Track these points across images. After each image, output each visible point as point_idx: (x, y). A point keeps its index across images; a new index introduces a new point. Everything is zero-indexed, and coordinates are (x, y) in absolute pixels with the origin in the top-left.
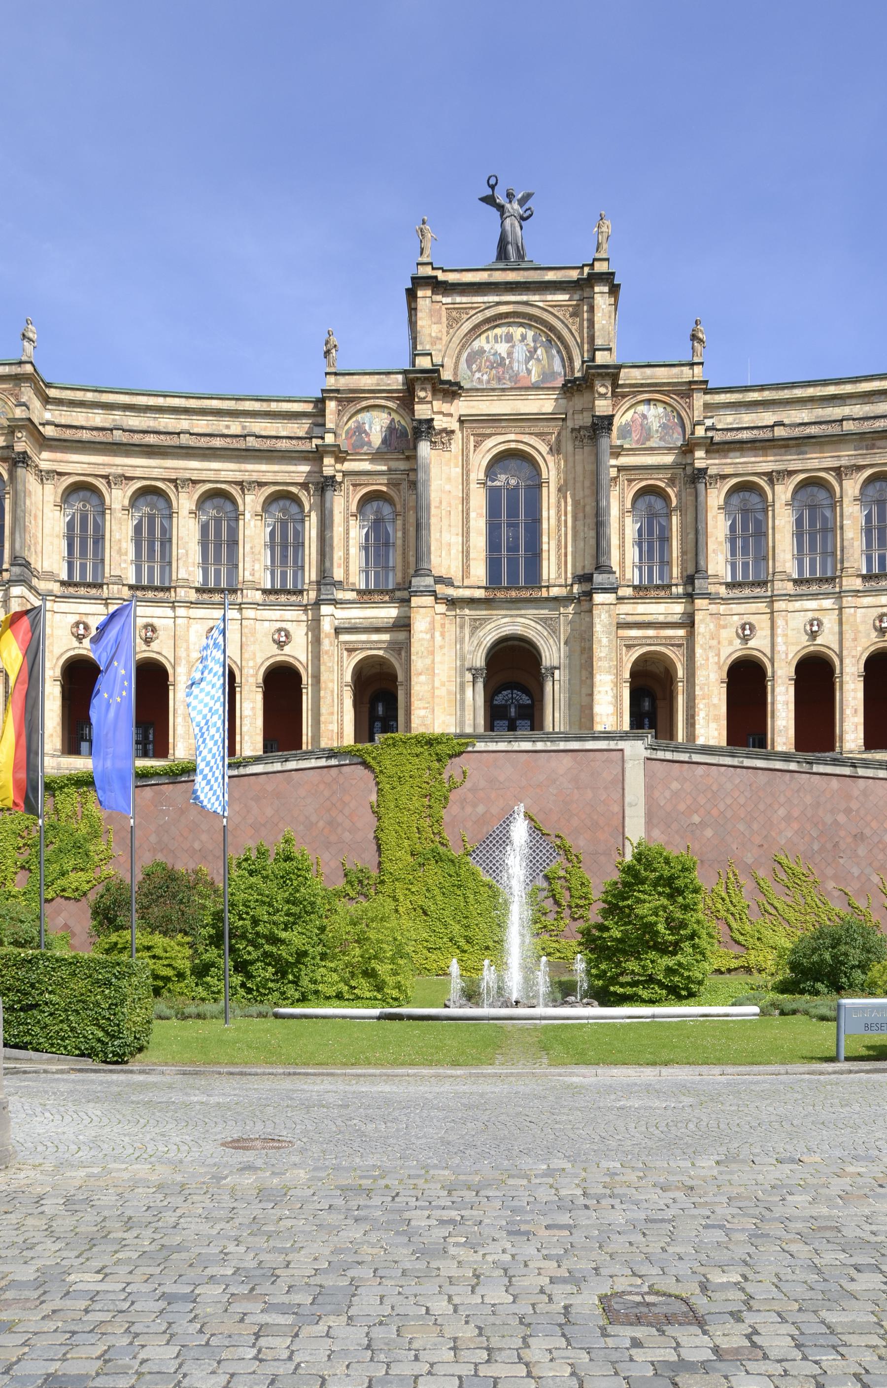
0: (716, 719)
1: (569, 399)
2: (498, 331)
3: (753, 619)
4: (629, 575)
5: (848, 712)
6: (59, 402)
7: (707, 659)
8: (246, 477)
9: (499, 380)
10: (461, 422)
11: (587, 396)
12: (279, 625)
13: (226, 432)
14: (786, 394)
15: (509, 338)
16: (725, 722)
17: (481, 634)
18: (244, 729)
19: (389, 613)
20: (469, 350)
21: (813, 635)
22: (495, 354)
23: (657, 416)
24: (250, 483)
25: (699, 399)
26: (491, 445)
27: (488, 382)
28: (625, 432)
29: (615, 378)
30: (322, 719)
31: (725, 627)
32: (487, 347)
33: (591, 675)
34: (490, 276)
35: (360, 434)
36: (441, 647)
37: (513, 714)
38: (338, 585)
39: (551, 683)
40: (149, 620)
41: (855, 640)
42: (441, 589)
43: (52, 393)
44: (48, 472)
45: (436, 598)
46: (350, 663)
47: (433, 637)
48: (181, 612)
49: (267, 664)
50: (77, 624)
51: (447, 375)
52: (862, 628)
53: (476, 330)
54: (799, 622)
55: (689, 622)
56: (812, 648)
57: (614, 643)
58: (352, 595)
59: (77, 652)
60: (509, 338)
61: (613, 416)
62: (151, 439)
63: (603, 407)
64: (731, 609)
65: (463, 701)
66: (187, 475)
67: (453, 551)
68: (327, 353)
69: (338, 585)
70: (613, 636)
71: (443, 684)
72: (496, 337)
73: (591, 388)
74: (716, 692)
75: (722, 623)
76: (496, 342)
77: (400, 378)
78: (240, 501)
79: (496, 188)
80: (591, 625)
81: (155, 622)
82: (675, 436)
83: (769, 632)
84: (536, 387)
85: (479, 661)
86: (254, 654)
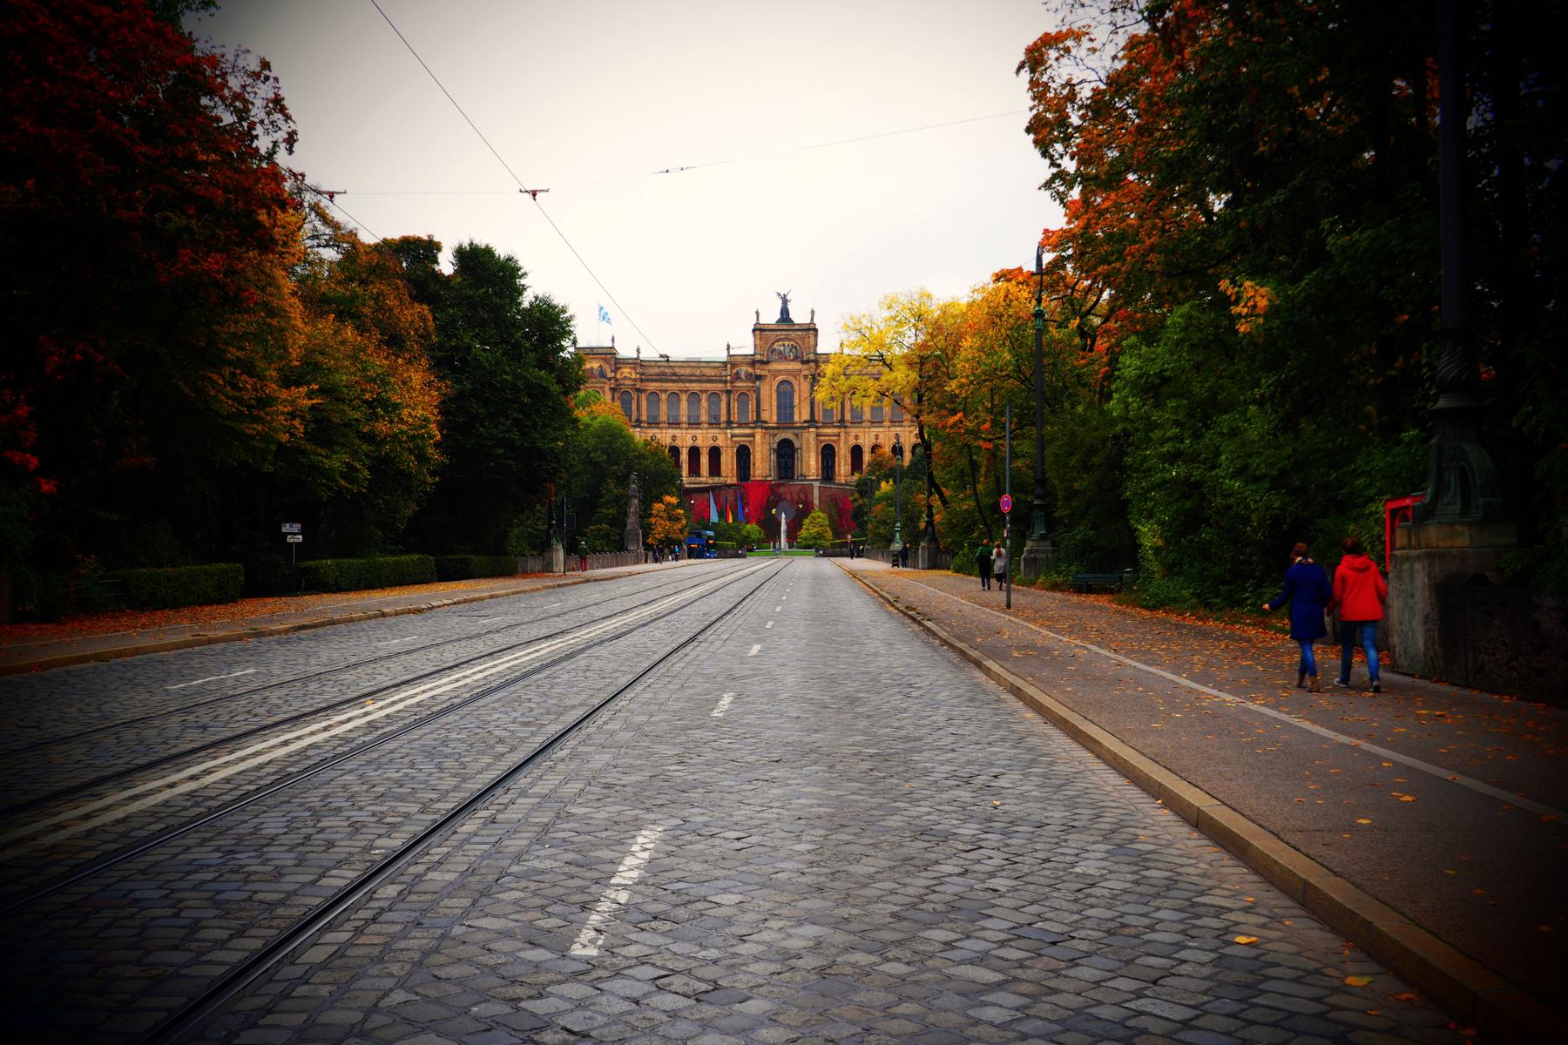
19: (747, 431)
21: (877, 439)
38: (732, 422)
53: (773, 343)
54: (872, 435)
68: (728, 349)
69: (732, 422)
85: (775, 446)
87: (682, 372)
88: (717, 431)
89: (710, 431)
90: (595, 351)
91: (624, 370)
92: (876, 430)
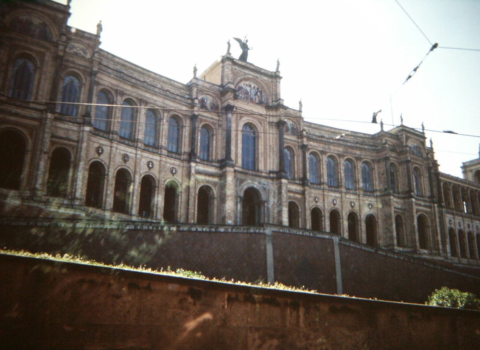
1: (267, 112)
2: (247, 83)
3: (319, 196)
9: (247, 99)
12: (172, 166)
15: (250, 86)
20: (238, 86)
21: (335, 204)
23: (290, 125)
27: (244, 98)
32: (244, 87)
34: (246, 65)
35: (203, 103)
40: (125, 153)
48: (139, 152)
53: (241, 81)
54: (330, 199)
55: (303, 193)
56: (334, 209)
60: (250, 86)
81: (128, 154)
84: (257, 104)
85: (242, 194)
88: (177, 162)
91: (76, 45)
92: (333, 194)
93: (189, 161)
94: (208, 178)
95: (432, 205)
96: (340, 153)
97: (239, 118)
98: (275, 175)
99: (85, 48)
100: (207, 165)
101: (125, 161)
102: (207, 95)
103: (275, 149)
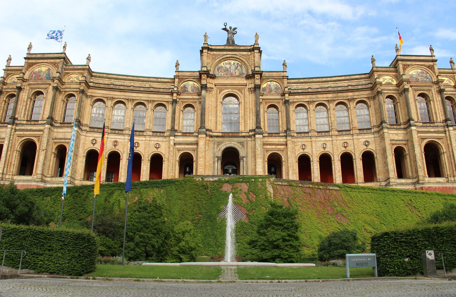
0: (295, 174)
2: (227, 62)
3: (305, 143)
4: (266, 130)
5: (337, 172)
6: (95, 77)
7: (292, 155)
8: (150, 99)
9: (227, 74)
10: (215, 85)
11: (253, 79)
12: (156, 142)
13: (145, 86)
14: (311, 80)
15: (230, 63)
16: (298, 175)
17: (220, 146)
18: (144, 174)
22: (225, 68)
24: (151, 101)
25: (285, 81)
26: (224, 92)
27: (223, 75)
28: (264, 89)
29: (261, 74)
30: (169, 171)
31: (297, 146)
32: (223, 66)
33: (255, 159)
35: (185, 88)
36: (208, 150)
37: (230, 172)
39: (242, 162)
40: (116, 140)
41: (337, 150)
42: (208, 133)
43: (94, 74)
44: (90, 96)
45: (206, 135)
46: (179, 155)
47: (205, 147)
49: (152, 154)
50: (93, 140)
51: (211, 73)
52: (339, 146)
53: (220, 61)
54: (320, 144)
56: (324, 152)
57: (262, 150)
58: (180, 134)
59: (92, 148)
60: (230, 63)
61: (261, 85)
62: (122, 88)
63: (258, 82)
64: (298, 140)
65: (214, 167)
66: (132, 98)
67: (212, 122)
68: (176, 66)
69: (176, 131)
70: (262, 148)
71: (208, 161)
72: (226, 63)
73: (254, 77)
74: (295, 165)
75: (296, 144)
76: (226, 64)
77: (198, 73)
78: (147, 106)
79: (227, 26)
80: (255, 145)
81: (118, 140)
82: (279, 91)
83: (311, 147)
84: (238, 76)
85: (220, 154)
86: (149, 151)
87: (132, 84)
88: (160, 139)
89: (153, 139)
90: (46, 56)
92: (323, 139)
93: (170, 136)
94: (187, 146)
95: (447, 129)
96: (329, 99)
97: (218, 93)
98: (253, 133)
99: (78, 76)
100: (189, 136)
101: (115, 146)
102: (188, 82)
103: (253, 110)
